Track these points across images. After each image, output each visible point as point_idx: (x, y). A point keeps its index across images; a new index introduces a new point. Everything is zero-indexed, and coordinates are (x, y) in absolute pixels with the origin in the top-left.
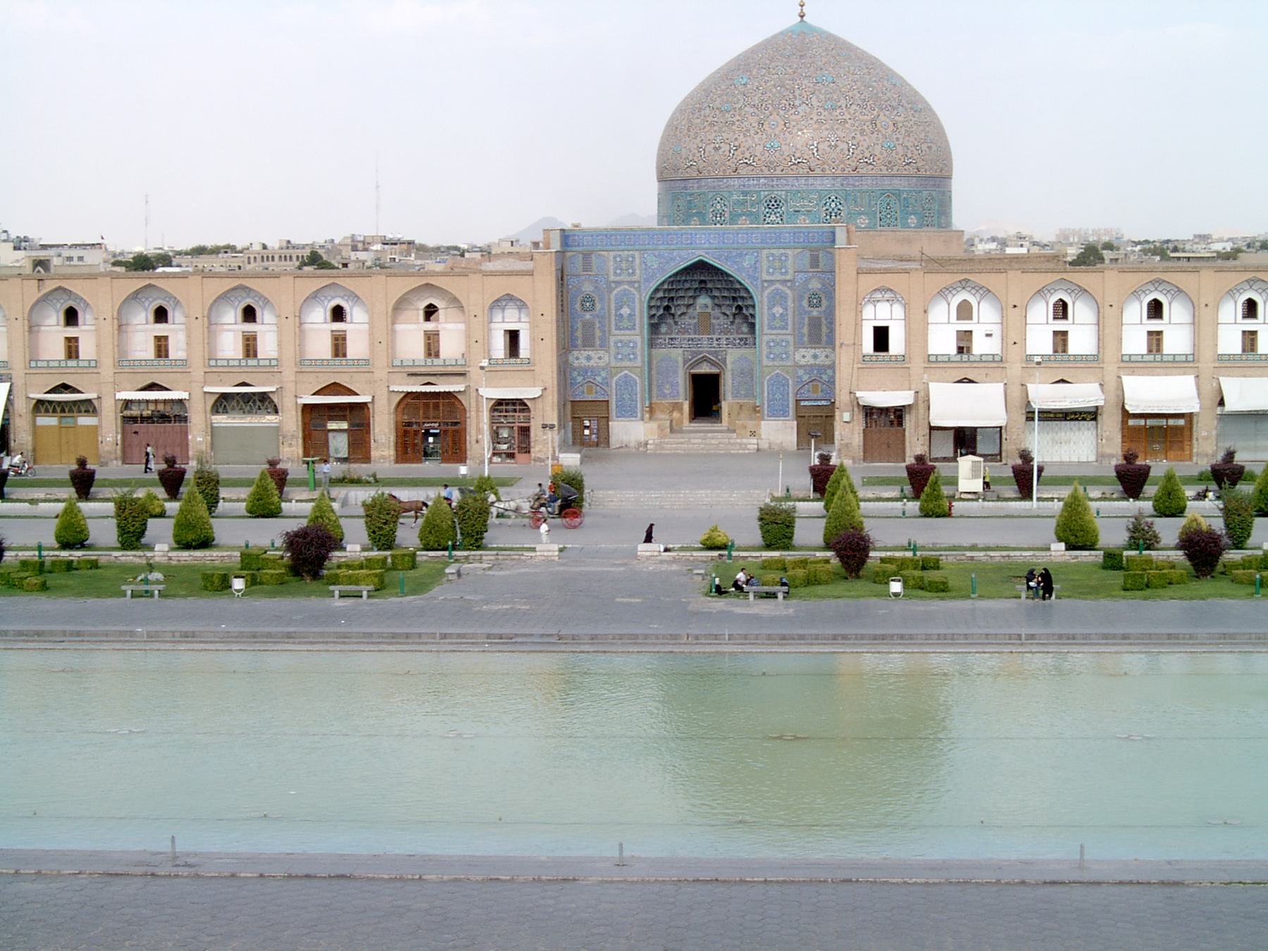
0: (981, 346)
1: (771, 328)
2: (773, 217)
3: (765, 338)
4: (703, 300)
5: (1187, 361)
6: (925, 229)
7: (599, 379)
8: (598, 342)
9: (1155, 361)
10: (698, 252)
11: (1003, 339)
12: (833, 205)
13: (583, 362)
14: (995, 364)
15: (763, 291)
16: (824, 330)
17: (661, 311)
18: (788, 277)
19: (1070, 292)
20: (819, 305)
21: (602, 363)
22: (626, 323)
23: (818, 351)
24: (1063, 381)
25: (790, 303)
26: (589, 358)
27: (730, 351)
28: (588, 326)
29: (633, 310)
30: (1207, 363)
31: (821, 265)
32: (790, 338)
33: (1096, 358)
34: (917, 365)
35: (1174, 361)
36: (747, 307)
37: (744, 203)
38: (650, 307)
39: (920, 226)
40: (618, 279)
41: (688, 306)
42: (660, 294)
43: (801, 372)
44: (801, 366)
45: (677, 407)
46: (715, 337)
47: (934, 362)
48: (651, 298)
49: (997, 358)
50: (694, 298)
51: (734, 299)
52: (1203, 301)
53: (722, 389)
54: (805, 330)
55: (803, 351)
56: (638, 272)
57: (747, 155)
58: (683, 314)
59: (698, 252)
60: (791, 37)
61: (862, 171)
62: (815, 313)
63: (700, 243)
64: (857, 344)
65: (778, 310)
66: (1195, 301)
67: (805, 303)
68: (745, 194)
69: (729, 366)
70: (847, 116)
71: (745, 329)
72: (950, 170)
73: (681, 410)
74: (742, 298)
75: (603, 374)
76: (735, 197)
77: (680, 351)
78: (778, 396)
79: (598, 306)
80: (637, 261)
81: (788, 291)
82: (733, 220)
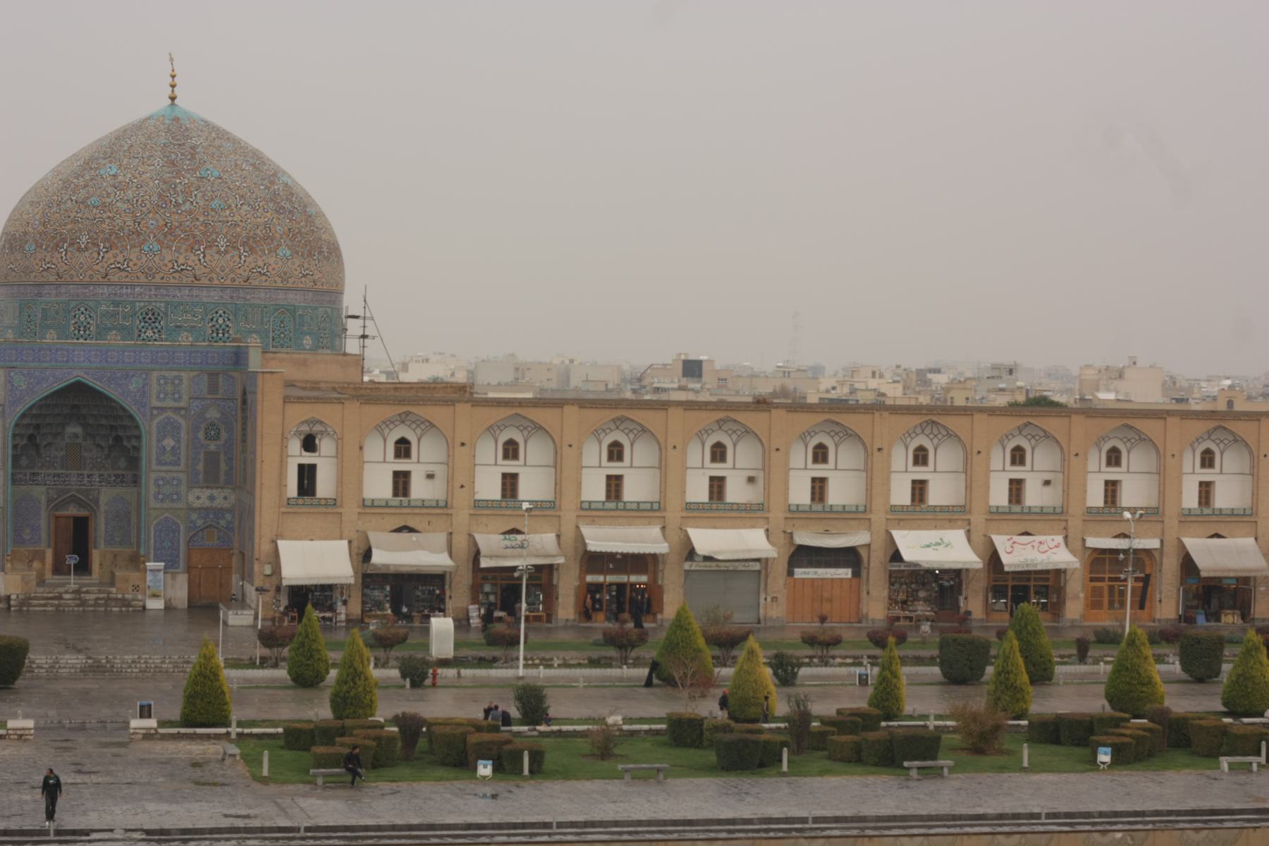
0: (420, 489)
1: (160, 463)
2: (149, 333)
3: (153, 476)
4: (74, 429)
5: (652, 510)
6: (320, 351)
9: (617, 509)
10: (75, 373)
11: (450, 481)
12: (221, 321)
14: (442, 508)
15: (151, 420)
16: (223, 466)
17: (25, 441)
18: (182, 404)
19: (522, 428)
20: (216, 438)
23: (215, 492)
24: (1217, 536)
25: (183, 435)
27: (104, 490)
30: (674, 513)
31: (221, 391)
32: (183, 476)
33: (761, 507)
34: (350, 510)
35: (638, 510)
36: (129, 438)
37: (114, 315)
38: (14, 436)
39: (316, 348)
41: (56, 435)
42: (27, 421)
43: (194, 516)
45: (40, 556)
46: (86, 472)
47: (369, 507)
48: (17, 425)
49: (442, 504)
51: (112, 427)
52: (877, 445)
53: (92, 535)
54: (200, 467)
55: (197, 492)
57: (120, 259)
58: (49, 444)
59: (75, 373)
60: (164, 124)
61: (256, 283)
62: (212, 447)
63: (81, 365)
64: (282, 485)
65: (169, 443)
66: (661, 440)
67: (201, 435)
68: (116, 304)
69: (103, 508)
70: (237, 218)
71: (122, 463)
72: (343, 285)
73: (43, 561)
74: (124, 428)
76: (104, 308)
77: (43, 489)
82: (102, 332)
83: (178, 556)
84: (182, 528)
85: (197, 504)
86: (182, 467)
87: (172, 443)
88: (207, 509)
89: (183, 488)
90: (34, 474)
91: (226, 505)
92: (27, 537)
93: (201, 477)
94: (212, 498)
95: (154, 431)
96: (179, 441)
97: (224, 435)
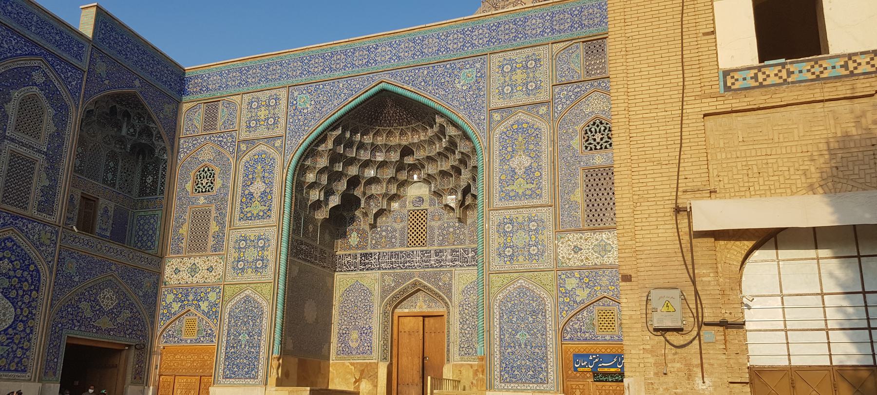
3: (496, 217)
7: (204, 306)
8: (211, 242)
13: (185, 277)
21: (212, 279)
22: (257, 208)
26: (194, 270)
28: (201, 219)
29: (270, 184)
32: (546, 214)
40: (252, 136)
50: (403, 184)
56: (282, 121)
65: (522, 161)
69: (457, 297)
75: (212, 296)
77: (377, 274)
79: (218, 183)
81: (544, 127)
83: (544, 358)
85: (575, 261)
86: (546, 199)
87: (526, 161)
88: (595, 268)
89: (548, 233)
90: (365, 255)
92: (354, 345)
95: (496, 146)
96: (537, 157)
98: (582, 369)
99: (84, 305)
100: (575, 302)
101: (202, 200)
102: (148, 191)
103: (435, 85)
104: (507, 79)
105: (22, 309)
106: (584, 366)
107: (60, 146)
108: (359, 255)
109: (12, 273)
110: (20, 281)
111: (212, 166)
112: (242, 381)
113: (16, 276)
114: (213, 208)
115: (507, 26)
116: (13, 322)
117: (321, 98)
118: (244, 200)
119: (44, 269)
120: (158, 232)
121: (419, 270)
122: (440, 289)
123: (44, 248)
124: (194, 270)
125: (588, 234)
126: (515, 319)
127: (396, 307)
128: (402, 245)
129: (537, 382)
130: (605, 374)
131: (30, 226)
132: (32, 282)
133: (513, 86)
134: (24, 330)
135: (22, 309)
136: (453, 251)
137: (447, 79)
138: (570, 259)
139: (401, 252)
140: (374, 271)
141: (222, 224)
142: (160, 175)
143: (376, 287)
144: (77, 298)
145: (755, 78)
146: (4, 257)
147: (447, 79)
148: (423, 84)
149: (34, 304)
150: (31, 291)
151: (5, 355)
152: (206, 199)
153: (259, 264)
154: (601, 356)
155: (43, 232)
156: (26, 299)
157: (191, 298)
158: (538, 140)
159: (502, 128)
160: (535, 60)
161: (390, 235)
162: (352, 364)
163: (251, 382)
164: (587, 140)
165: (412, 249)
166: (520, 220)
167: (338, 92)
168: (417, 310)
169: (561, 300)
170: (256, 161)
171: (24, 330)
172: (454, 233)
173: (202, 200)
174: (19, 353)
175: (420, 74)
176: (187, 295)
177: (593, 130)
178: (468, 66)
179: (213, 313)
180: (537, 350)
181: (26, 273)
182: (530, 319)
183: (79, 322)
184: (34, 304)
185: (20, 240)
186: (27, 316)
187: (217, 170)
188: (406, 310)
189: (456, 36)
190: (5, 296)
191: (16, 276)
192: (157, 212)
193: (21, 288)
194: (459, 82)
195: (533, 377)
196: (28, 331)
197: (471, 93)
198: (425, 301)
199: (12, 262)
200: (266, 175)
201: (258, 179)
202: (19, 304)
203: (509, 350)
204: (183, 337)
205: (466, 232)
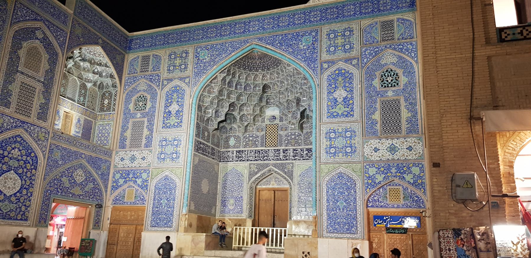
1: (332, 115)
3: (324, 129)
7: (139, 181)
8: (144, 141)
18: (354, 53)
21: (144, 164)
22: (173, 120)
26: (133, 159)
40: (171, 76)
44: (372, 164)
54: (377, 116)
55: (374, 143)
65: (340, 94)
67: (376, 83)
75: (144, 176)
78: (341, 204)
80: (191, 56)
81: (355, 72)
83: (355, 218)
84: (359, 185)
85: (375, 157)
87: (344, 94)
89: (358, 140)
90: (239, 152)
91: (412, 156)
93: (378, 127)
94: (393, 149)
97: (403, 80)
98: (379, 225)
99: (64, 179)
100: (375, 183)
101: (139, 115)
102: (105, 109)
103: (287, 46)
104: (332, 42)
105: (26, 181)
106: (380, 224)
107: (52, 78)
108: (235, 152)
109: (20, 158)
110: (25, 163)
111: (145, 94)
112: (163, 229)
113: (22, 160)
114: (146, 119)
115: (332, 10)
116: (20, 189)
117: (215, 53)
118: (165, 115)
119: (40, 155)
120: (111, 135)
121: (272, 162)
122: (285, 174)
123: (41, 142)
124: (133, 159)
125: (383, 140)
126: (336, 193)
127: (257, 184)
128: (262, 146)
129: (351, 233)
130: (394, 229)
131: (32, 128)
132: (33, 164)
133: (336, 47)
134: (27, 194)
135: (26, 181)
136: (294, 150)
137: (294, 42)
138: (372, 156)
139: (262, 150)
140: (244, 162)
141: (151, 130)
142: (113, 99)
143: (246, 172)
144: (60, 175)
145: (521, 33)
146: (15, 147)
147: (294, 42)
148: (279, 45)
149: (33, 178)
150: (32, 169)
151: (14, 210)
152: (141, 114)
153: (174, 156)
154: (391, 217)
155: (40, 132)
156: (29, 174)
157: (131, 176)
158: (351, 80)
159: (328, 73)
160: (350, 31)
161: (255, 140)
162: (230, 219)
163: (168, 229)
164: (383, 81)
165: (268, 148)
166: (340, 131)
167: (225, 49)
168: (271, 186)
169: (366, 181)
170: (174, 92)
171: (27, 194)
172: (295, 138)
173: (139, 115)
174: (23, 208)
175: (277, 39)
176: (129, 175)
177: (386, 74)
178: (307, 34)
179: (144, 186)
180: (350, 213)
181: (29, 158)
182: (346, 193)
183: (61, 190)
184: (33, 178)
185: (26, 136)
186: (29, 185)
187: (149, 97)
188: (264, 187)
189: (299, 16)
190: (15, 172)
191: (22, 160)
192: (111, 122)
193: (25, 167)
194: (302, 44)
195: (348, 229)
196: (29, 195)
197: (309, 51)
198: (276, 181)
199: (20, 150)
200: (180, 100)
201: (174, 103)
202: (24, 177)
203: (333, 213)
204: (125, 201)
205: (302, 138)
